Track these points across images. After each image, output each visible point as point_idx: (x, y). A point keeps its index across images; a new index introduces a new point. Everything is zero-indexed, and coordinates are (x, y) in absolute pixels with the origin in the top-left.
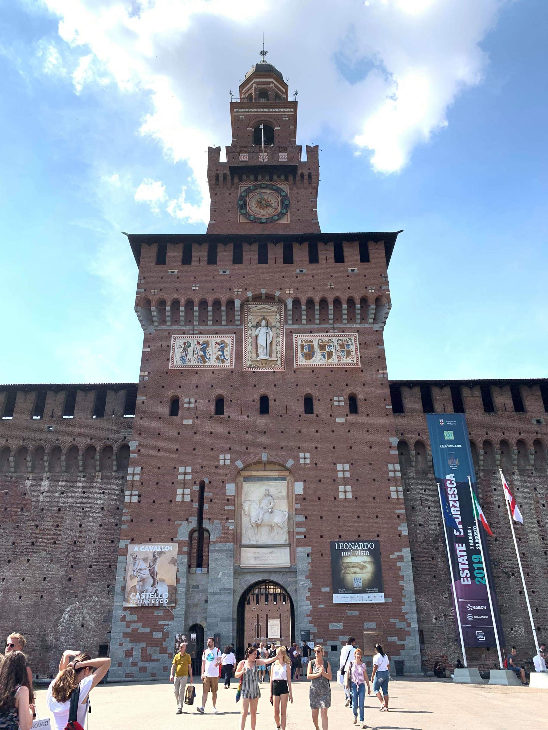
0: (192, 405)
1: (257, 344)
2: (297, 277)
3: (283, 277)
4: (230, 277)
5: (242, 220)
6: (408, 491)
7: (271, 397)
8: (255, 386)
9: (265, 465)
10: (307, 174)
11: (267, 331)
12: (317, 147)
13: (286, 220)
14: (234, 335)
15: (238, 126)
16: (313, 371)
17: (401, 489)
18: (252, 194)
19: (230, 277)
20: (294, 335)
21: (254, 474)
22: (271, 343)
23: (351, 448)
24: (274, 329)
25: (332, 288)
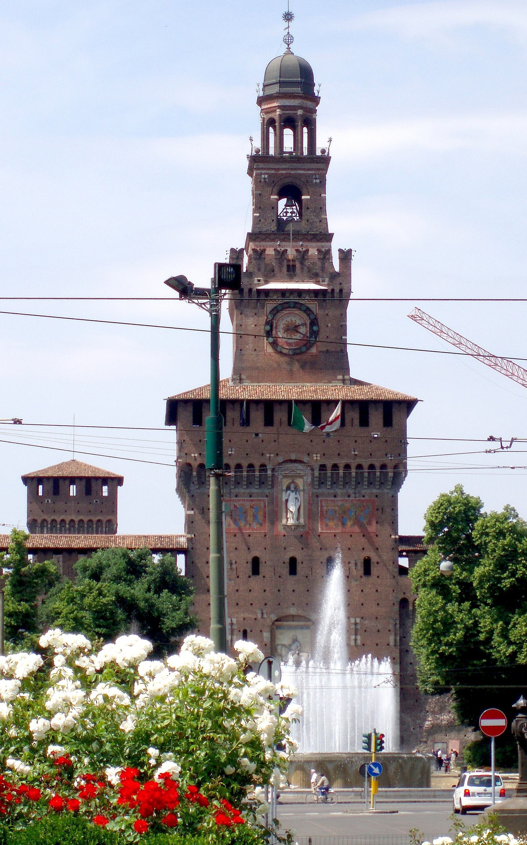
0: (234, 566)
1: (287, 509)
2: (324, 441)
3: (311, 441)
4: (263, 441)
5: (270, 350)
6: (405, 637)
7: (299, 559)
8: (285, 549)
9: (293, 618)
10: (338, 291)
11: (296, 496)
12: (350, 251)
13: (314, 350)
14: (266, 499)
15: (260, 192)
16: (335, 536)
17: (398, 638)
18: (279, 315)
19: (263, 441)
20: (320, 499)
21: (285, 623)
22: (299, 509)
23: (362, 604)
24: (302, 493)
25: (356, 455)
